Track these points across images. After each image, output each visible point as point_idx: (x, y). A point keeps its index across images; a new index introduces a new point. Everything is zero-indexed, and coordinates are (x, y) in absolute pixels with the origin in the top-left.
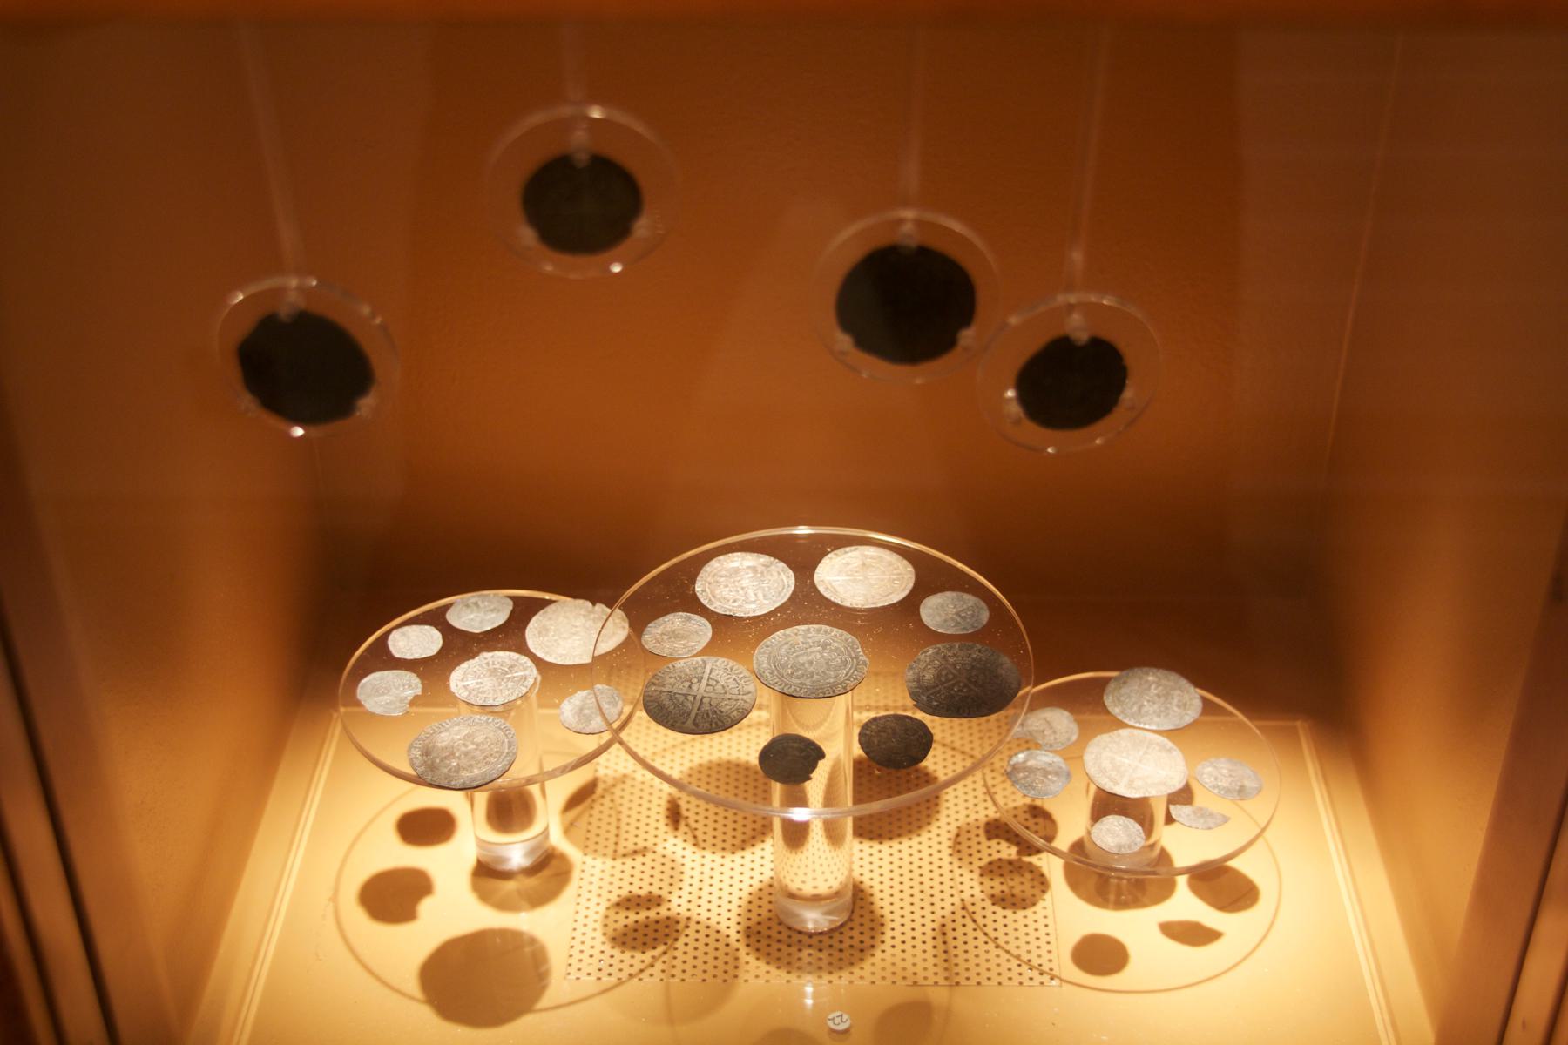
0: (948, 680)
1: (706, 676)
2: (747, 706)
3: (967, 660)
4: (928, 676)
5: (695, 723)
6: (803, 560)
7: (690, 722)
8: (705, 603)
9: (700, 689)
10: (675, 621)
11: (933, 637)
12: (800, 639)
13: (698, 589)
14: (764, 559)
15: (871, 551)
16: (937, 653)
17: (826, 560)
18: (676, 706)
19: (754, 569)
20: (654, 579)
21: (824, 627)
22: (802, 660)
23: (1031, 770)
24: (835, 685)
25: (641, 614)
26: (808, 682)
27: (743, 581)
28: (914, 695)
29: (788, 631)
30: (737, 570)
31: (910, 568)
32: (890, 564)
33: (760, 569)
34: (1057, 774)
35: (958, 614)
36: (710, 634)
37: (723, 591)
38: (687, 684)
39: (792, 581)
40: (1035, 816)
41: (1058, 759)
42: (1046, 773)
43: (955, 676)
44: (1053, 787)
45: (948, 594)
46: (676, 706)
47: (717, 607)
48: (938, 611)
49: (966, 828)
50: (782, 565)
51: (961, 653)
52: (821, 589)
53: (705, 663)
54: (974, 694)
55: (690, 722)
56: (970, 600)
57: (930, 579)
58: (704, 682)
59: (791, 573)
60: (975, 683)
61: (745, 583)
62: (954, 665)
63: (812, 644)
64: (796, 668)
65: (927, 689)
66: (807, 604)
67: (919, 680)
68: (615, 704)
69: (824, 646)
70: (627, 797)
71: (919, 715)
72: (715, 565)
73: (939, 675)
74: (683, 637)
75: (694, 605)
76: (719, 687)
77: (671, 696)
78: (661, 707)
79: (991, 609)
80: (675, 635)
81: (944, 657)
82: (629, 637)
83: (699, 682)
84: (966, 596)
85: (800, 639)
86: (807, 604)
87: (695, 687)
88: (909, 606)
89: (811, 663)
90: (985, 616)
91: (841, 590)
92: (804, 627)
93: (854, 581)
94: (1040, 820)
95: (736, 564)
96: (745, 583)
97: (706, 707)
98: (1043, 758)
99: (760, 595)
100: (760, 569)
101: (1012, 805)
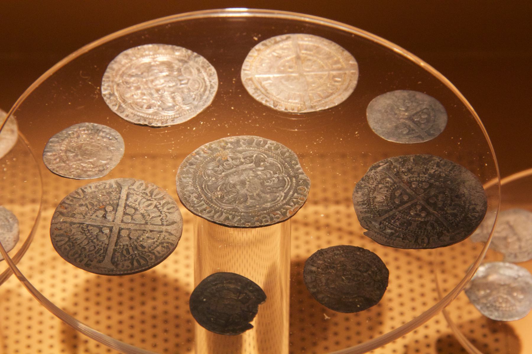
0: (403, 203)
1: (122, 203)
2: (173, 238)
3: (424, 177)
4: (380, 198)
5: (114, 262)
6: (226, 48)
7: (107, 259)
8: (114, 109)
9: (116, 218)
10: (81, 134)
11: (384, 149)
12: (229, 154)
13: (105, 92)
14: (180, 52)
15: (306, 40)
16: (389, 169)
17: (253, 53)
18: (90, 241)
19: (169, 65)
20: (50, 78)
21: (257, 138)
22: (233, 180)
23: (492, 287)
24: (273, 210)
25: (39, 122)
26: (241, 208)
27: (157, 81)
28: (364, 221)
29: (214, 144)
30: (149, 68)
31: (353, 62)
32: (329, 56)
33: (176, 65)
34: (523, 290)
35: (410, 118)
36: (122, 150)
37: (134, 95)
38: (101, 213)
39: (215, 80)
40: (494, 331)
41: (523, 272)
42: (510, 290)
43: (411, 198)
44: (519, 308)
45: (398, 93)
46: (90, 241)
47: (128, 114)
48: (389, 114)
49: (413, 346)
50: (202, 59)
51: (416, 169)
52: (250, 90)
53: (120, 187)
54: (436, 218)
55: (107, 259)
56: (424, 100)
57: (376, 74)
58: (121, 209)
59: (213, 70)
60: (434, 205)
61: (160, 83)
62: (409, 183)
63: (243, 158)
64: (227, 188)
65: (380, 213)
66: (234, 105)
67: (368, 202)
68: (10, 230)
69: (258, 162)
70: (14, 318)
71: (370, 246)
72: (123, 61)
73: (392, 197)
74: (91, 155)
75: (100, 112)
76: (138, 217)
77: (84, 229)
78: (72, 242)
79: (449, 110)
80: (82, 152)
81: (397, 174)
82: (19, 142)
83: (115, 210)
84: (420, 96)
85: (229, 154)
86: (234, 105)
87: (110, 217)
88: (353, 109)
89: (243, 183)
90: (442, 121)
91: (273, 91)
92: (233, 139)
93: (288, 79)
94: (500, 336)
95: (146, 60)
96: (160, 83)
97: (125, 241)
98: (507, 272)
99: (179, 98)
100: (176, 65)
101: (466, 317)
